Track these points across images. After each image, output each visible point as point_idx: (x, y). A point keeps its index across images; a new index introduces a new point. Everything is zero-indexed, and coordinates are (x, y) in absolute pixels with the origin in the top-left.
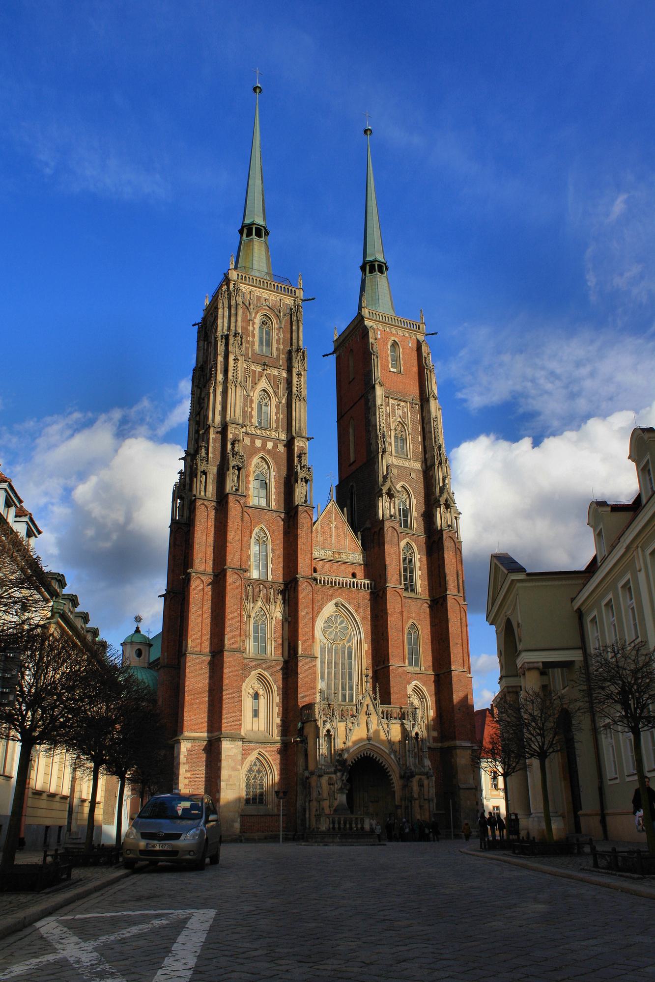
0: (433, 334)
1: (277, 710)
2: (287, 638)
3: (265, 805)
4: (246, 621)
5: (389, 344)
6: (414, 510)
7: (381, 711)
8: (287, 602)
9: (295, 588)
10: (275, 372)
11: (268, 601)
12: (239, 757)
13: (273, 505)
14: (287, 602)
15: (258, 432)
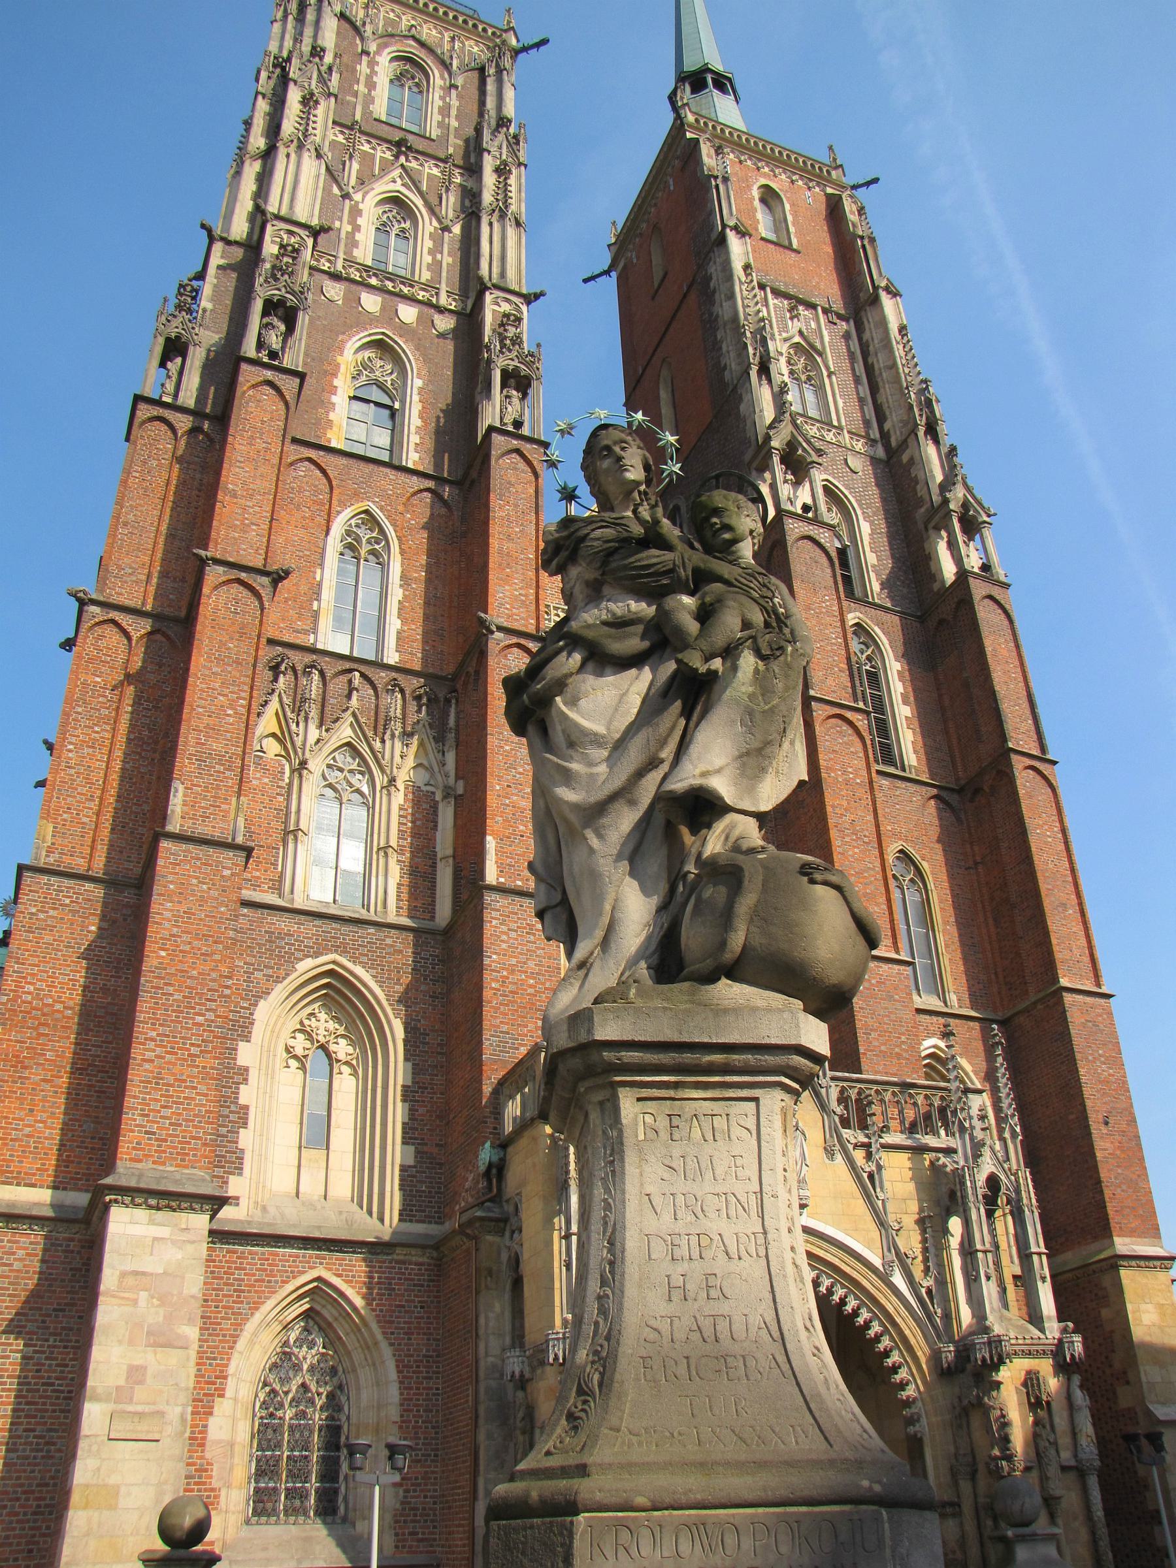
0: (868, 184)
1: (397, 1113)
2: (450, 852)
3: (345, 1520)
4: (290, 785)
5: (756, 193)
6: (867, 549)
7: (834, 1093)
8: (451, 736)
9: (477, 672)
10: (431, 170)
11: (380, 724)
12: (194, 1284)
13: (412, 458)
14: (451, 736)
15: (374, 281)
